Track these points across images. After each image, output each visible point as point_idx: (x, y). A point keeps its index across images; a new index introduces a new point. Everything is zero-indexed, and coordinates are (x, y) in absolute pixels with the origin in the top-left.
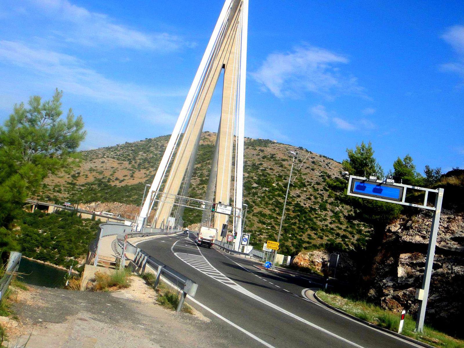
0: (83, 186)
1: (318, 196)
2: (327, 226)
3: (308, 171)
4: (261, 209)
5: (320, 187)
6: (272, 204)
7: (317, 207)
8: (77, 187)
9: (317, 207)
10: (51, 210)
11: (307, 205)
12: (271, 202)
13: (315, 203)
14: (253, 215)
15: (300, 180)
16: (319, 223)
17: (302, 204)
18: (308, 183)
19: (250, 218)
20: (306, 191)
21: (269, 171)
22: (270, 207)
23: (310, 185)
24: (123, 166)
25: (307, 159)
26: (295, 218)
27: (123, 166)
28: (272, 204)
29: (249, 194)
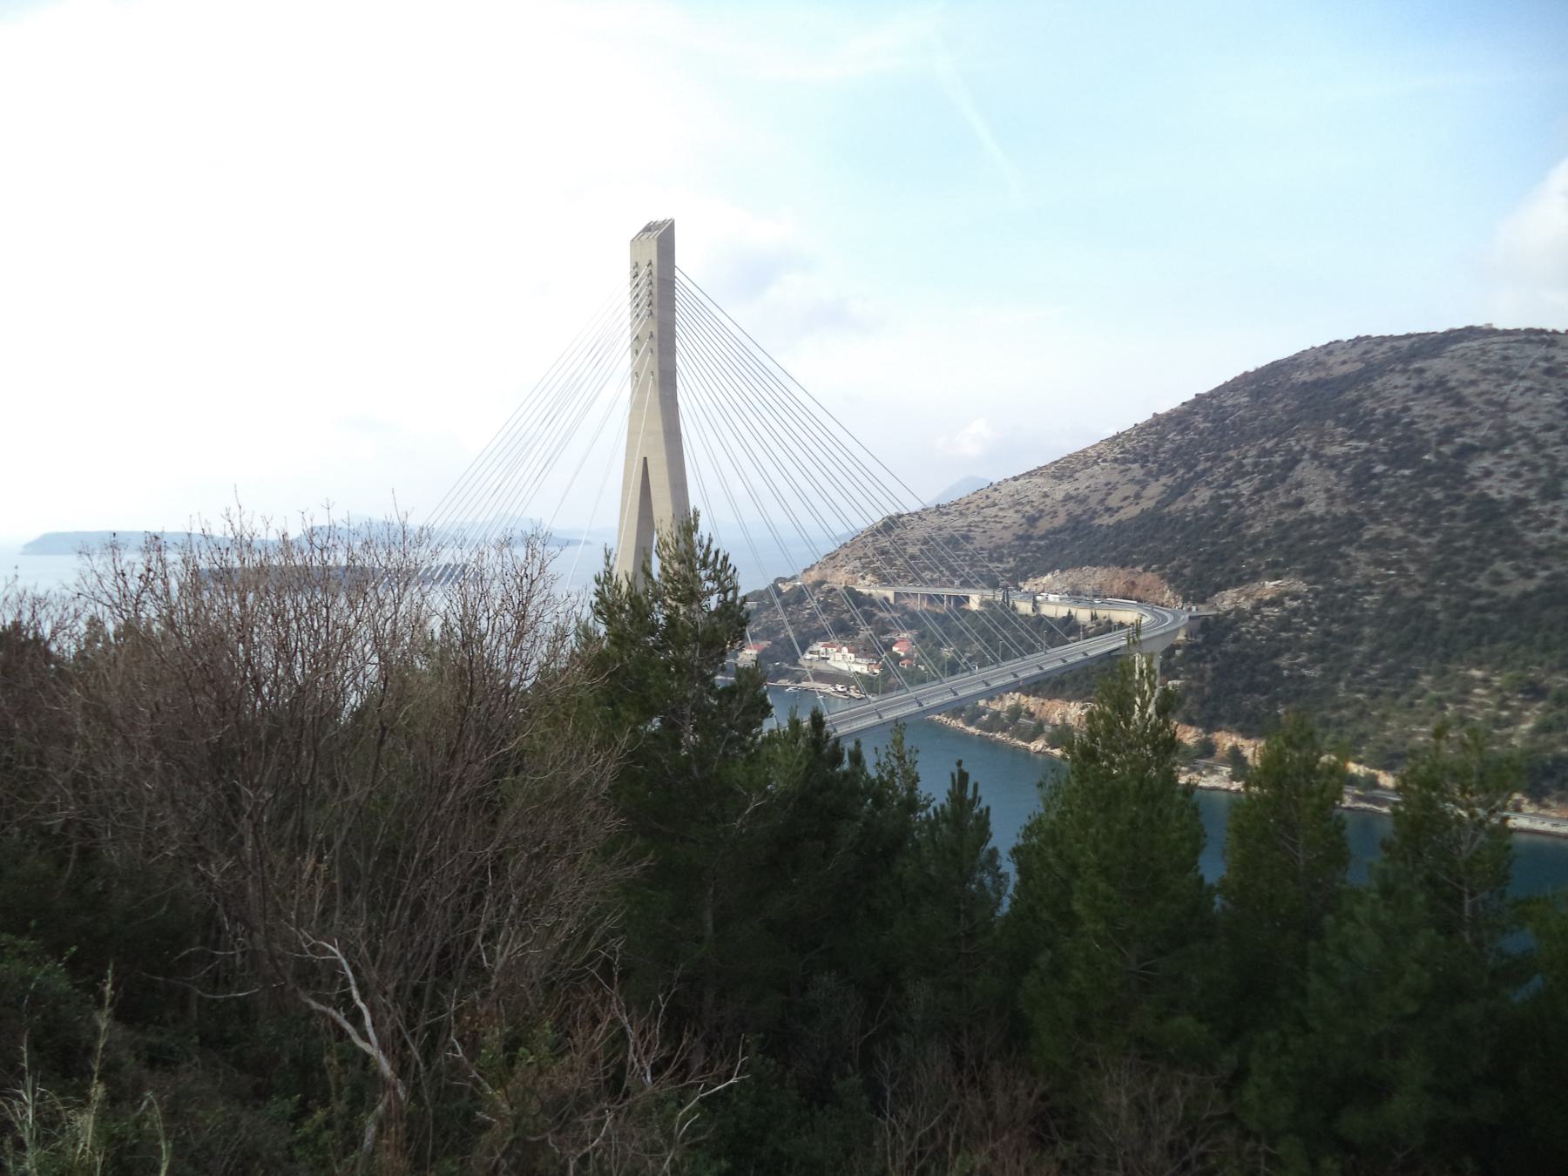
0: (1042, 538)
1: (1542, 462)
2: (1552, 539)
3: (1528, 398)
4: (1380, 528)
5: (1552, 436)
6: (1413, 511)
7: (1531, 493)
8: (1032, 543)
9: (1531, 493)
10: (974, 604)
11: (1508, 493)
12: (1409, 505)
13: (1529, 485)
14: (1361, 548)
15: (1501, 429)
16: (1531, 536)
17: (1493, 494)
18: (1520, 434)
19: (1348, 556)
20: (1509, 457)
21: (1421, 426)
22: (1406, 518)
23: (1526, 436)
24: (1129, 476)
25: (1533, 366)
26: (1465, 535)
27: (1129, 476)
28: (1413, 511)
29: (1361, 494)
